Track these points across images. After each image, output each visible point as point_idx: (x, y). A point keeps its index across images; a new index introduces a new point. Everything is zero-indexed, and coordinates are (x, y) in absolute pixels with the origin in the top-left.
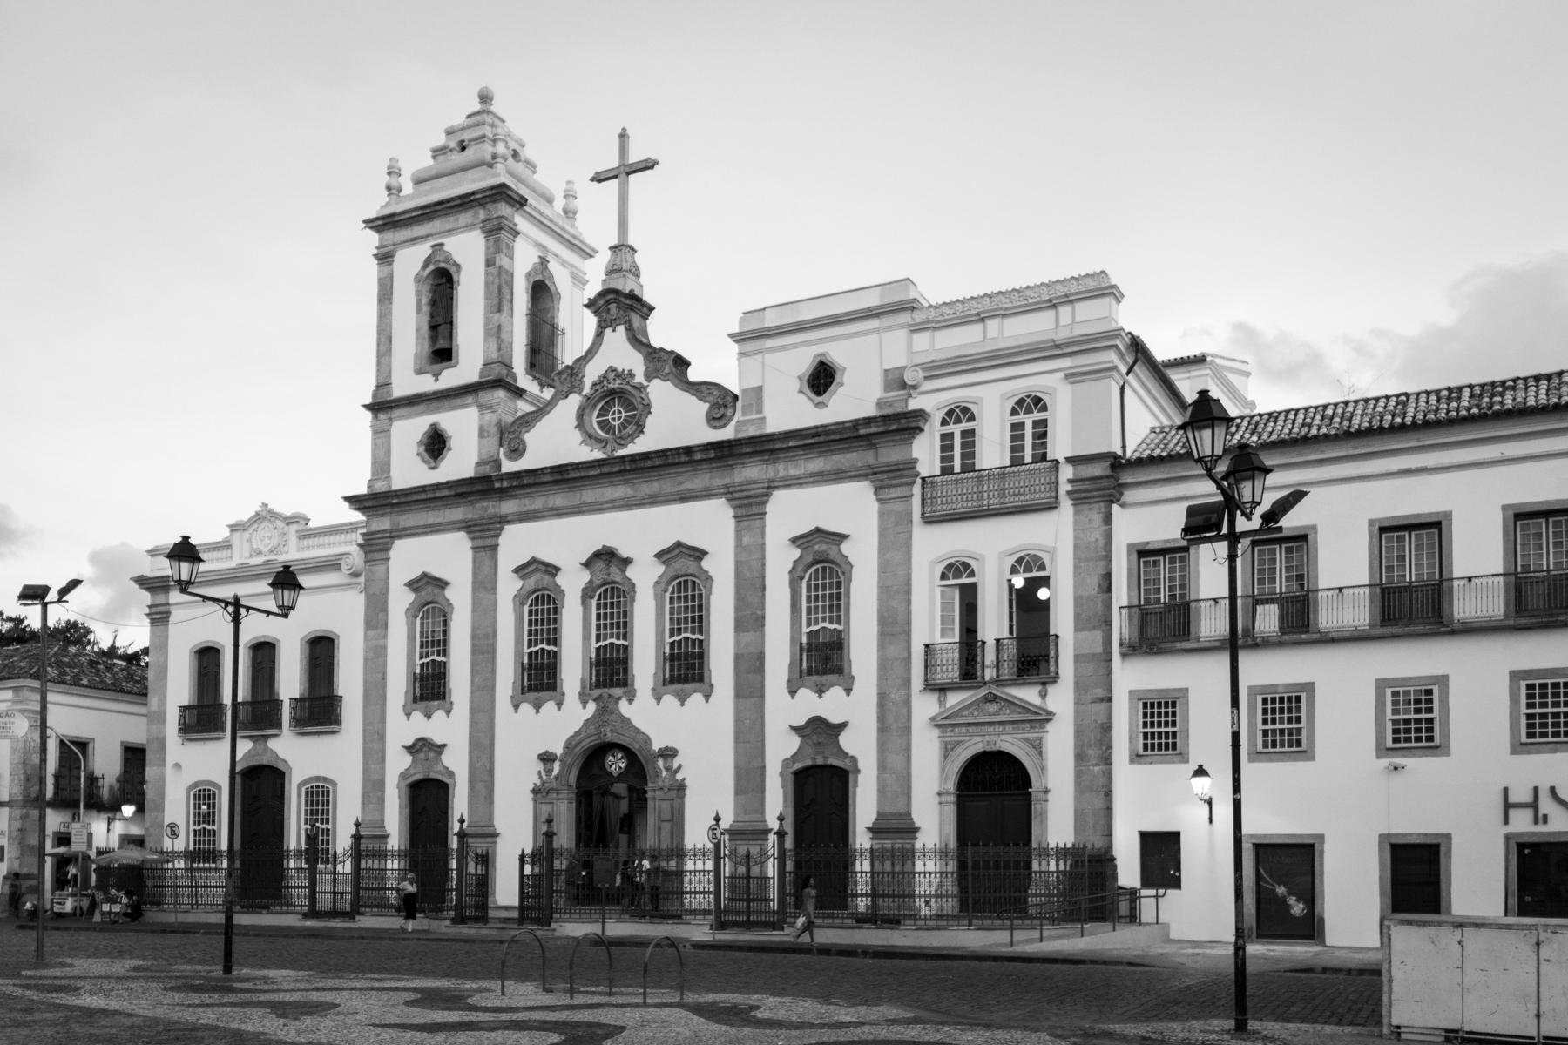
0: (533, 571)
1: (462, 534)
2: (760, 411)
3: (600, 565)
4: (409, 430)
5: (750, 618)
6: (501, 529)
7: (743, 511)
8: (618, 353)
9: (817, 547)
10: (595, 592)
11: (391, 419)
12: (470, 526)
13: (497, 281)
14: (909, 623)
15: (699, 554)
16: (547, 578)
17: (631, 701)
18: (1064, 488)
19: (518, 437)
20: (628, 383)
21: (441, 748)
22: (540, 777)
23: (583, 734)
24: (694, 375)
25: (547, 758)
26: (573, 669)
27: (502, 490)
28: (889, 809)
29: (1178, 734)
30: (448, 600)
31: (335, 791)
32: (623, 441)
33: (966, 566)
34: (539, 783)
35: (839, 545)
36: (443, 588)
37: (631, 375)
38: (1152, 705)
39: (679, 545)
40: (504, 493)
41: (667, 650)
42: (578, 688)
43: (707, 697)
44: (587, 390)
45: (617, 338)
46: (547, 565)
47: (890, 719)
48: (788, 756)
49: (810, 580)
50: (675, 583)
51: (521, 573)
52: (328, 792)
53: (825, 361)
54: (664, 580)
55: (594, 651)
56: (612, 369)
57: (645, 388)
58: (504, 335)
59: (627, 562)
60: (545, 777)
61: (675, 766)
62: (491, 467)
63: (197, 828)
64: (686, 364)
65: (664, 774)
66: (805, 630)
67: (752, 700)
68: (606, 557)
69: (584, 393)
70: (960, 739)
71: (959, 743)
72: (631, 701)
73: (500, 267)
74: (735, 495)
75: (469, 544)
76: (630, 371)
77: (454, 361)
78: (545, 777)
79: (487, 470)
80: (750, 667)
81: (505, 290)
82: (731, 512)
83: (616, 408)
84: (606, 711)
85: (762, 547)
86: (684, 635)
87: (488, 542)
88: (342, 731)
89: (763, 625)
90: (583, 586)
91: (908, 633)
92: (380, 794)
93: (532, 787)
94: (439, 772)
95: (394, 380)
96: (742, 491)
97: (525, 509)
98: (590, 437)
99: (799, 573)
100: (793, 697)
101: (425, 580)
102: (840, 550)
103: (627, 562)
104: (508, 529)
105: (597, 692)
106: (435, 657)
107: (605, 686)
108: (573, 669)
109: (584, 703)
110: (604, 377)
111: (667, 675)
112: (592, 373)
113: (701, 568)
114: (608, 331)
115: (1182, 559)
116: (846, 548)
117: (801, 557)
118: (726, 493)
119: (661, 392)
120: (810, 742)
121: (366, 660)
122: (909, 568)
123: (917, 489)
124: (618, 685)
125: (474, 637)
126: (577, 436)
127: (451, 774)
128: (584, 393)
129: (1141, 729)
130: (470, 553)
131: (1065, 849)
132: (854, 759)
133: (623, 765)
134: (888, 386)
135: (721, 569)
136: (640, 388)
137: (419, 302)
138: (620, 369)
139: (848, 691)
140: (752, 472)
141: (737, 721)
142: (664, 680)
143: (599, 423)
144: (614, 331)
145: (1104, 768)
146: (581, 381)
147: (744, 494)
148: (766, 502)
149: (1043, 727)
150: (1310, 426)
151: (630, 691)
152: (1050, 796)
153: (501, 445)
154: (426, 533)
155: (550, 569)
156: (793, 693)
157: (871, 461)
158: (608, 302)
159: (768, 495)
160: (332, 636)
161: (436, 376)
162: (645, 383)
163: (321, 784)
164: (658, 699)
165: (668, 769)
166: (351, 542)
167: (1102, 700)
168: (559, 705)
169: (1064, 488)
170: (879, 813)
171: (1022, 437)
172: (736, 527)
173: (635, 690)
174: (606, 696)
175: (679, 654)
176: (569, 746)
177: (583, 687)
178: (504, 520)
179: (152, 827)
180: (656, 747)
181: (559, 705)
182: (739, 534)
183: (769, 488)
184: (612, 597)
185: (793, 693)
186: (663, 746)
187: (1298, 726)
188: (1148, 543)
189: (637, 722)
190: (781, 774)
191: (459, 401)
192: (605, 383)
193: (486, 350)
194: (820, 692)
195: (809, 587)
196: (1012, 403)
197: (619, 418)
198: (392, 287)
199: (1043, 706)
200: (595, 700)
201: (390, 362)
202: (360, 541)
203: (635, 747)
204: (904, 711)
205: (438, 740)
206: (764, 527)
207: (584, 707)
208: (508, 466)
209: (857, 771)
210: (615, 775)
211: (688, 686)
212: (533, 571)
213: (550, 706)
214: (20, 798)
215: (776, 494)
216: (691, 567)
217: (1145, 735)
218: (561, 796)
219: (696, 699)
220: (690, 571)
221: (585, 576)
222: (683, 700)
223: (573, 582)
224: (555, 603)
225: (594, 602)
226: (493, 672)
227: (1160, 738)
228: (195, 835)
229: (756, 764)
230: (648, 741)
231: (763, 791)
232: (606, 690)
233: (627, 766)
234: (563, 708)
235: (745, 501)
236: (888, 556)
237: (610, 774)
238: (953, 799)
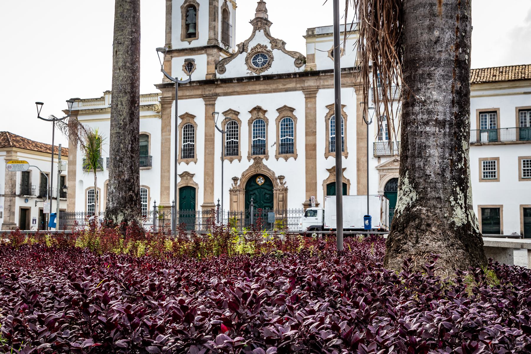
0: (229, 113)
1: (201, 99)
2: (314, 62)
3: (255, 112)
4: (178, 62)
5: (311, 132)
6: (217, 98)
7: (308, 96)
8: (261, 39)
10: (253, 121)
11: (172, 57)
12: (204, 97)
13: (214, 10)
15: (292, 110)
16: (234, 116)
17: (267, 159)
19: (223, 66)
20: (265, 50)
21: (192, 175)
22: (233, 186)
23: (249, 171)
24: (288, 48)
25: (235, 179)
26: (245, 147)
27: (217, 85)
30: (195, 123)
31: (149, 191)
32: (262, 70)
34: (232, 188)
36: (193, 118)
37: (266, 47)
39: (285, 106)
40: (218, 86)
41: (280, 142)
42: (247, 155)
43: (295, 159)
44: (249, 51)
45: (260, 34)
46: (235, 111)
49: (332, 119)
50: (283, 119)
51: (225, 114)
52: (146, 191)
54: (279, 118)
55: (252, 142)
56: (259, 45)
57: (271, 52)
58: (216, 29)
59: (265, 111)
60: (234, 186)
61: (284, 182)
62: (212, 76)
63: (90, 204)
64: (284, 43)
65: (280, 185)
67: (312, 160)
68: (258, 109)
69: (248, 52)
72: (267, 159)
73: (215, 6)
74: (305, 90)
75: (204, 103)
76: (266, 45)
77: (197, 37)
78: (234, 186)
79: (211, 77)
80: (311, 149)
81: (216, 13)
82: (304, 96)
83: (260, 58)
84: (258, 162)
85: (315, 108)
86: (286, 137)
87: (211, 102)
88: (152, 169)
89: (316, 135)
90: (249, 119)
92: (168, 191)
93: (229, 189)
94: (192, 184)
95: (173, 43)
96: (308, 89)
97: (226, 91)
98: (250, 67)
99: (328, 117)
101: (186, 115)
103: (265, 111)
104: (219, 98)
105: (254, 156)
106: (189, 143)
107: (257, 154)
108: (245, 147)
109: (249, 160)
110: (256, 47)
111: (280, 151)
112: (252, 45)
113: (265, 117)
114: (257, 31)
117: (329, 112)
118: (302, 89)
119: (276, 53)
121: (162, 143)
124: (262, 154)
125: (206, 135)
126: (246, 67)
127: (197, 184)
128: (248, 52)
130: (204, 107)
133: (263, 182)
135: (300, 115)
136: (269, 52)
137: (182, 15)
138: (262, 45)
140: (311, 82)
141: (306, 167)
142: (279, 152)
143: (253, 62)
144: (260, 31)
146: (247, 48)
147: (309, 90)
150: (495, 76)
151: (267, 156)
153: (216, 68)
154: (186, 98)
155: (236, 113)
157: (354, 81)
158: (257, 22)
159: (317, 91)
160: (147, 134)
161: (190, 43)
162: (271, 50)
163: (143, 188)
164: (277, 159)
165: (281, 183)
166: (155, 100)
168: (240, 160)
172: (306, 101)
173: (269, 156)
174: (258, 158)
175: (284, 144)
176: (243, 175)
177: (249, 154)
178: (217, 95)
179: (70, 204)
180: (277, 175)
181: (240, 160)
182: (306, 103)
183: (317, 88)
184: (259, 123)
186: (280, 175)
189: (269, 167)
191: (199, 52)
192: (256, 49)
193: (209, 35)
197: (261, 61)
198: (171, 9)
200: (254, 159)
201: (171, 36)
202: (160, 100)
203: (269, 175)
205: (192, 173)
206: (316, 101)
207: (249, 161)
208: (219, 76)
210: (260, 185)
211: (288, 155)
212: (229, 113)
213: (236, 161)
214: (10, 193)
215: (320, 91)
216: (289, 114)
218: (240, 192)
219: (291, 159)
220: (289, 115)
221: (250, 116)
222: (286, 159)
223: (245, 118)
224: (237, 125)
225: (252, 125)
226: (213, 148)
228: (89, 207)
230: (274, 173)
232: (257, 156)
233: (265, 182)
234: (241, 161)
235: (309, 93)
237: (258, 185)
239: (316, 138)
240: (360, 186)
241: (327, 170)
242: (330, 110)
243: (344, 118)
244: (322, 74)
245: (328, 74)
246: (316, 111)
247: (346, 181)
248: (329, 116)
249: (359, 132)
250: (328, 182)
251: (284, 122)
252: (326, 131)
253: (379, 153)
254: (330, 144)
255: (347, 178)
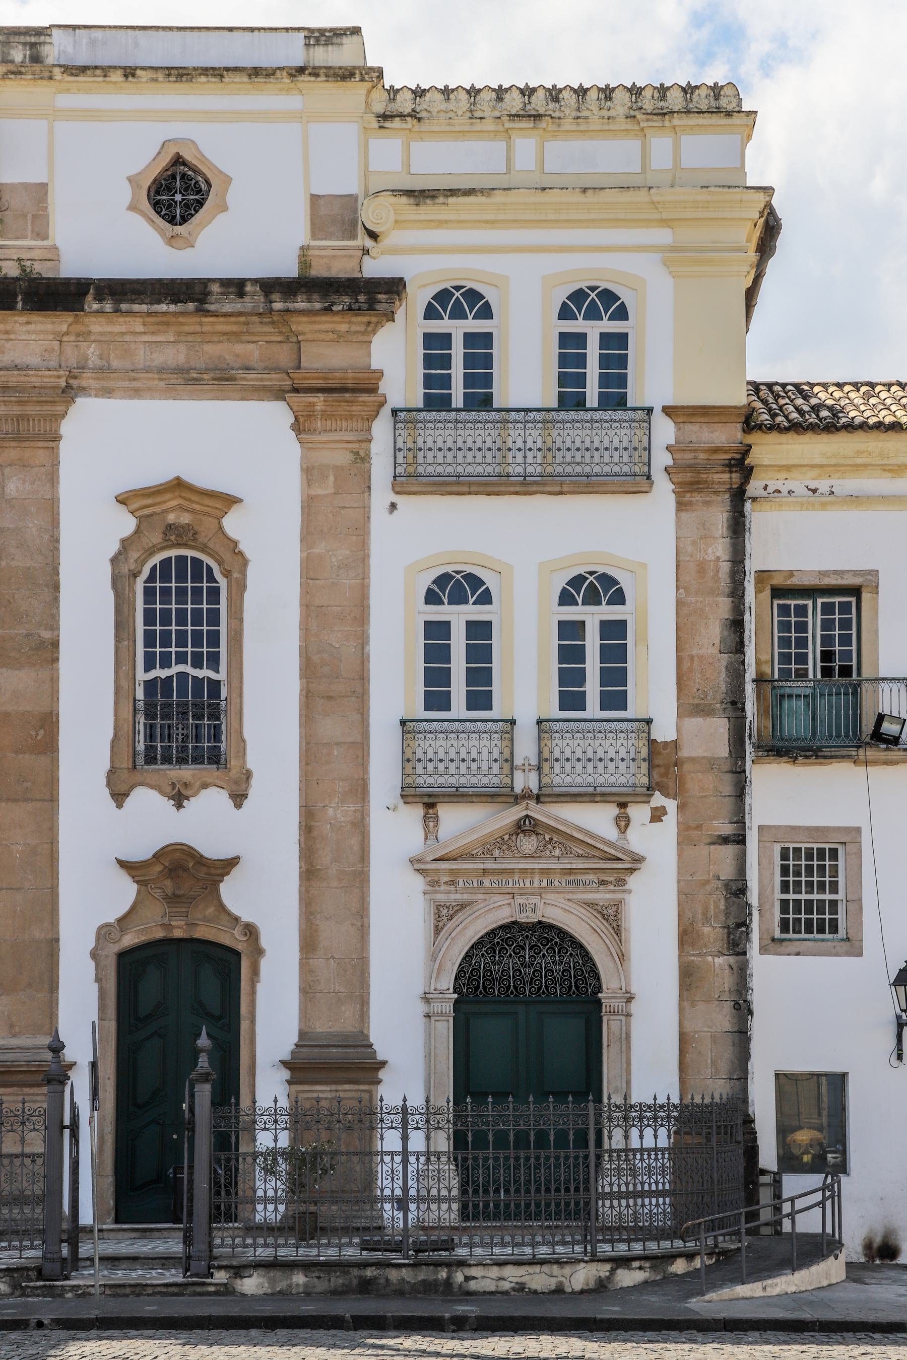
9: (171, 518)
14: (363, 677)
18: (661, 459)
28: (321, 1026)
29: (841, 908)
33: (475, 581)
35: (219, 519)
38: (821, 856)
47: (325, 857)
48: (111, 919)
49: (151, 578)
53: (188, 156)
66: (142, 676)
67: (29, 806)
70: (466, 897)
71: (462, 906)
91: (363, 698)
100: (119, 806)
102: (221, 528)
115: (845, 608)
116: (233, 524)
117: (138, 531)
120: (157, 893)
122: (365, 576)
123: (382, 428)
129: (779, 895)
131: (667, 1106)
132: (251, 931)
134: (318, 227)
139: (239, 798)
145: (732, 960)
148: (64, 415)
149: (621, 882)
152: (635, 1007)
156: (119, 797)
167: (725, 840)
169: (661, 459)
170: (302, 1034)
171: (581, 361)
185: (119, 797)
187: (833, 897)
188: (791, 574)
190: (94, 955)
194: (179, 799)
195: (149, 593)
196: (561, 295)
199: (620, 843)
204: (354, 841)
206: (56, 464)
209: (259, 952)
217: (784, 904)
227: (809, 911)
229: (39, 933)
231: (53, 987)
236: (320, 548)
238: (448, 1007)
239: (54, 681)
240: (318, 963)
241: (123, 864)
242: (140, 519)
243: (227, 574)
244: (95, 306)
245: (136, 307)
246: (55, 522)
247: (237, 932)
248: (134, 555)
249: (316, 658)
250: (129, 940)
251: (166, 577)
252: (118, 639)
253: (427, 780)
254: (141, 719)
255: (245, 918)
